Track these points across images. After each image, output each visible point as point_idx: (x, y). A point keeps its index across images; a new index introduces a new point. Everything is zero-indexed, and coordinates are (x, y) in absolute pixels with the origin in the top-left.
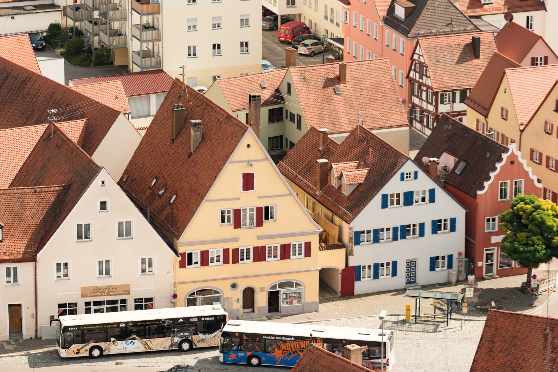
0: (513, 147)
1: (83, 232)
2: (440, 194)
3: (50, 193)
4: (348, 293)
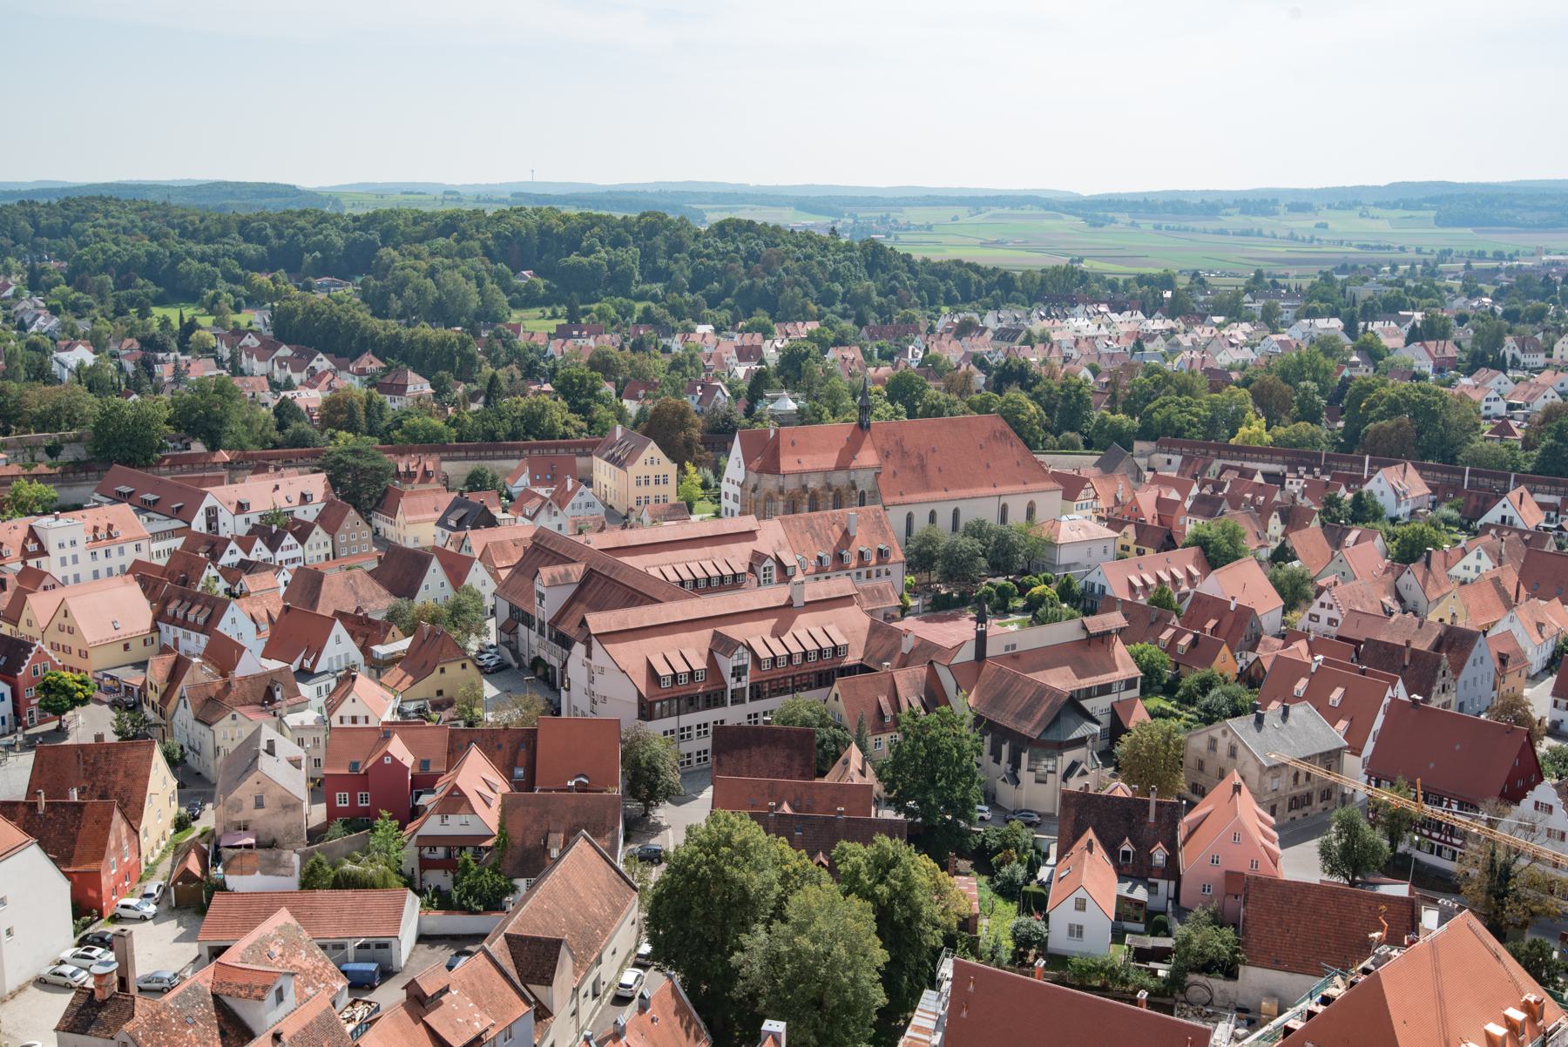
0: (38, 643)
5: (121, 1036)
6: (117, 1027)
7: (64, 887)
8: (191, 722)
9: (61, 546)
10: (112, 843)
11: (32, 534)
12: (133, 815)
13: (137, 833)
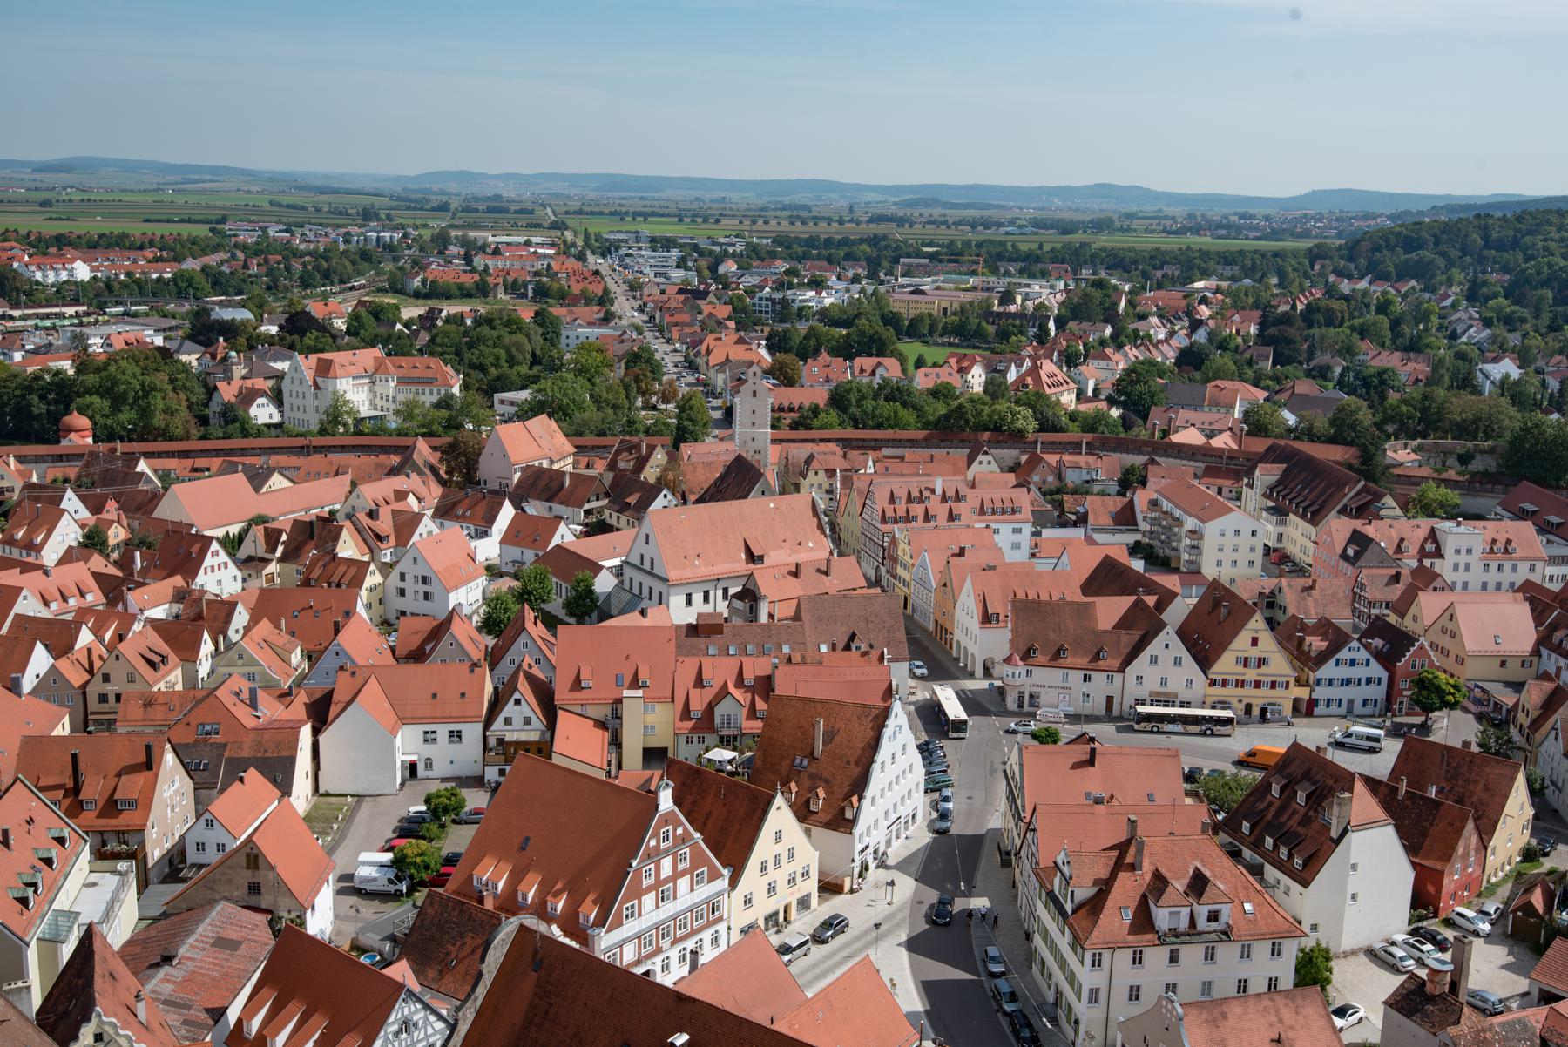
1: (1154, 660)
2: (1373, 662)
3: (1136, 635)
4: (1309, 714)
5: (1442, 1036)
6: (1442, 1028)
7: (1410, 875)
8: (1559, 756)
9: (1458, 551)
10: (1460, 850)
11: (1433, 535)
12: (1486, 831)
13: (1486, 848)
